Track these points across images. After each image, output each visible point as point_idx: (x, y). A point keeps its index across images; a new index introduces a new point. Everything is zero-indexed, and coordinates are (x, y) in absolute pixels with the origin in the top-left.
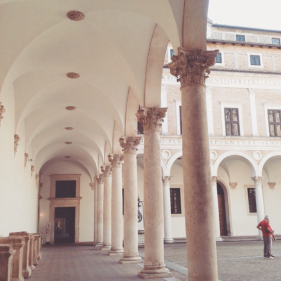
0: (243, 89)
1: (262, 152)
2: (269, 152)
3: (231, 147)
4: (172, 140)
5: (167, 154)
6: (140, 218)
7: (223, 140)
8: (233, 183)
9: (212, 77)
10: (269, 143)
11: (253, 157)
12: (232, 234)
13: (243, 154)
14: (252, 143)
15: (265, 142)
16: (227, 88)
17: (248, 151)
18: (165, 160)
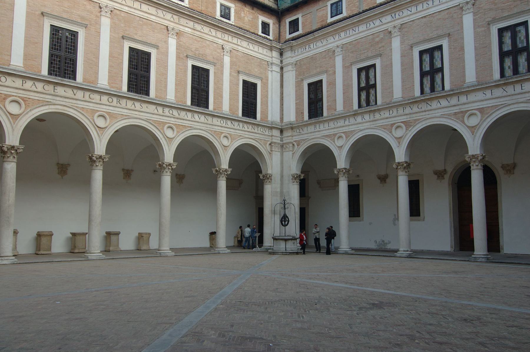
0: (451, 9)
1: (481, 110)
2: (496, 108)
3: (427, 113)
4: (347, 119)
5: (341, 139)
6: (286, 223)
7: (415, 105)
8: (508, 165)
9: (403, 9)
10: (498, 92)
11: (465, 124)
12: (503, 249)
13: (445, 120)
14: (463, 99)
15: (488, 92)
16: (425, 17)
17: (455, 114)
18: (339, 147)
